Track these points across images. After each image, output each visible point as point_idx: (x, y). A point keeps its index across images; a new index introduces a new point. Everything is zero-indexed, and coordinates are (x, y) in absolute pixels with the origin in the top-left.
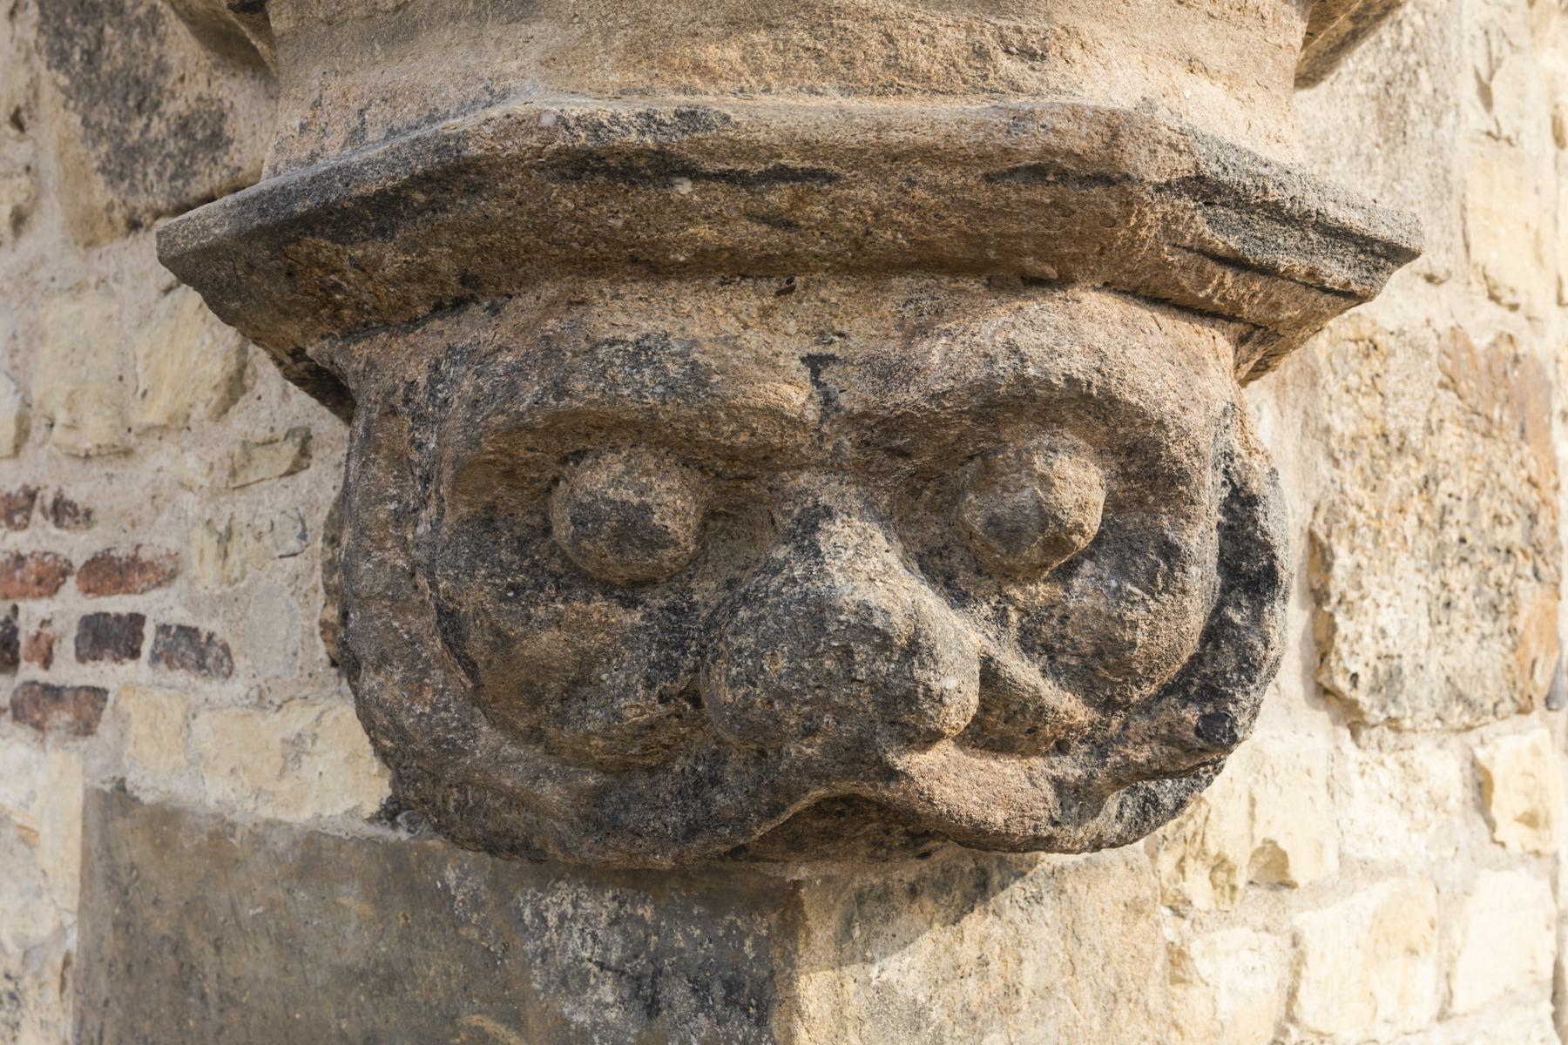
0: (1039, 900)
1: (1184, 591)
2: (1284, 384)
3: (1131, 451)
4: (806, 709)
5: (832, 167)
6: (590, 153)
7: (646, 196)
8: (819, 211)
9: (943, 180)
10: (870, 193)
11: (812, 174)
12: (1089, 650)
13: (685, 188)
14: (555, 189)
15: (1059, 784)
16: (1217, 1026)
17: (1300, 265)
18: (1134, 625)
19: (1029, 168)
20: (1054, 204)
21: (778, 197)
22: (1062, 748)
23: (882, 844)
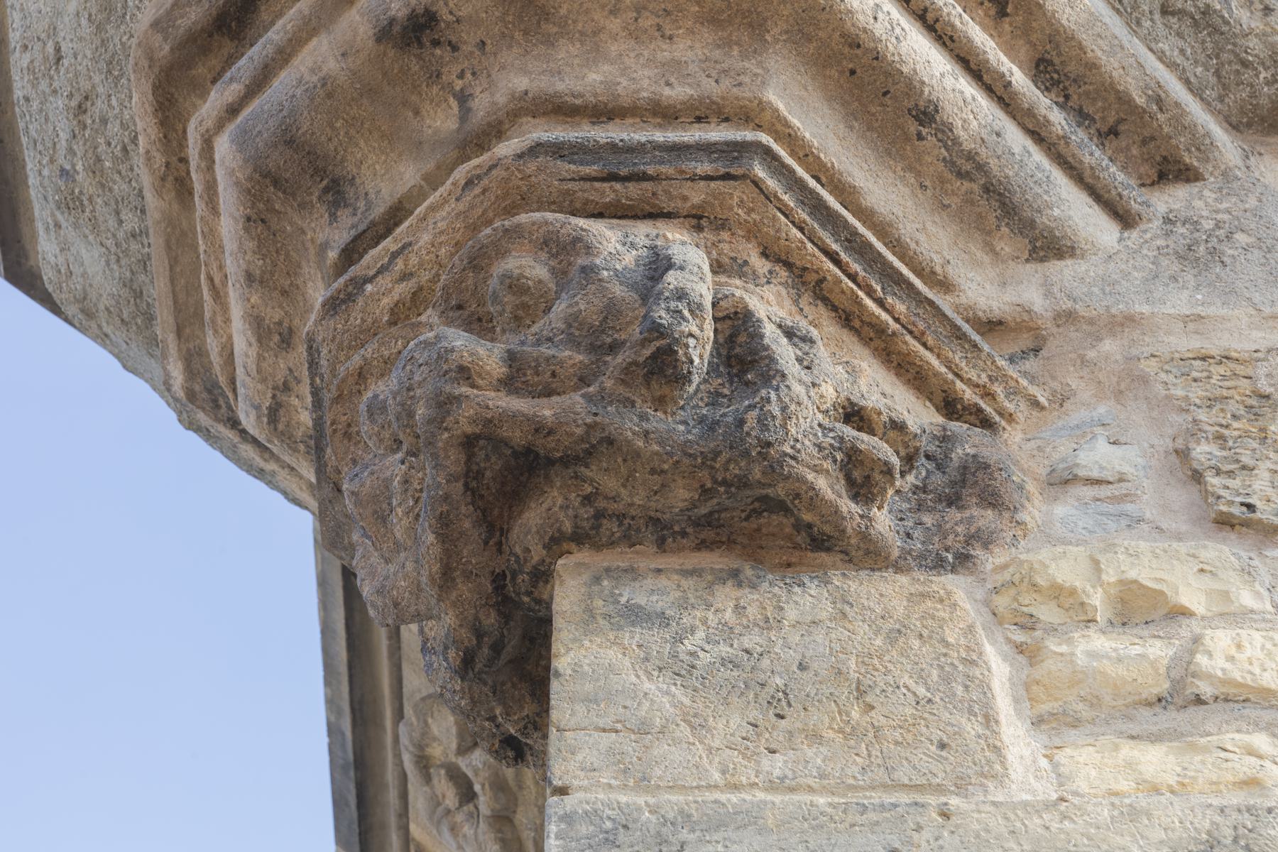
0: (802, 585)
1: (600, 280)
2: (1121, 392)
3: (546, 243)
4: (412, 393)
5: (406, 240)
6: (332, 297)
7: (360, 301)
8: (414, 260)
9: (444, 214)
10: (426, 238)
11: (404, 248)
12: (563, 326)
13: (369, 287)
14: (332, 322)
15: (583, 396)
16: (1081, 676)
17: (666, 169)
18: (577, 303)
19: (466, 184)
20: (483, 192)
21: (399, 265)
22: (584, 381)
23: (568, 507)
